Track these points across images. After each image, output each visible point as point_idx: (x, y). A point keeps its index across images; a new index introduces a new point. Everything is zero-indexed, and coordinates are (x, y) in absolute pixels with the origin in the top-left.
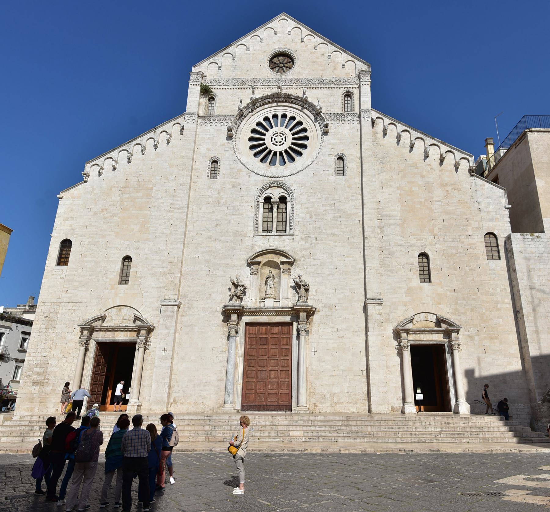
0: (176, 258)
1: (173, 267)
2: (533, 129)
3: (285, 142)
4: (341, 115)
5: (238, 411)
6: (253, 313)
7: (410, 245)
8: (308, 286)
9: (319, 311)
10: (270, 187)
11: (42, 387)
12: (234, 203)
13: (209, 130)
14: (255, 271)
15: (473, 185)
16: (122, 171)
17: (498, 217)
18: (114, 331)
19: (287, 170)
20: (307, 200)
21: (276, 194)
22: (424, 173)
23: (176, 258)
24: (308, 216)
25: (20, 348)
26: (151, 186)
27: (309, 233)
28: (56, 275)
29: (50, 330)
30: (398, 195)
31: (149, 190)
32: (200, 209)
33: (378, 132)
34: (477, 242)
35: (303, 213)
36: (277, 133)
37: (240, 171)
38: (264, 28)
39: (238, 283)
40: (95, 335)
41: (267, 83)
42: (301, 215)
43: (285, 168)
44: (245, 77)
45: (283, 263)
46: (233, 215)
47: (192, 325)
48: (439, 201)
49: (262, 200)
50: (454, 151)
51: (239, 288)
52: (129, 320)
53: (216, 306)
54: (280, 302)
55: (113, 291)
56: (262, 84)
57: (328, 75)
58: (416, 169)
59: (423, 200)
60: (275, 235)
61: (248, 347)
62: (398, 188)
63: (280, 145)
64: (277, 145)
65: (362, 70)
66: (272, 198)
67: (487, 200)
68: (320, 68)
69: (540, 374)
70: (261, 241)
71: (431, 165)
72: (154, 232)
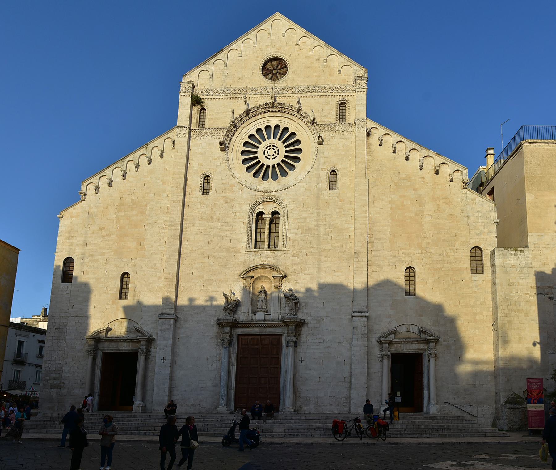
0: (171, 275)
1: (169, 283)
2: (529, 141)
3: (278, 155)
4: (335, 125)
5: (232, 412)
7: (398, 259)
8: (297, 300)
9: (307, 323)
10: (263, 202)
11: (59, 390)
12: (227, 219)
13: (201, 143)
14: (247, 286)
15: (465, 198)
16: (116, 189)
17: (486, 231)
18: (117, 342)
19: (279, 185)
20: (299, 216)
21: (267, 209)
22: (417, 187)
23: (171, 275)
25: (39, 355)
26: (145, 203)
27: (301, 248)
28: (62, 291)
29: (61, 341)
30: (390, 209)
31: (143, 208)
32: (193, 226)
33: (373, 144)
34: (463, 256)
36: (270, 146)
37: (232, 186)
38: (257, 30)
40: (101, 345)
41: (260, 92)
42: (292, 231)
43: (278, 183)
44: (236, 85)
48: (430, 215)
49: (255, 216)
50: (448, 163)
52: (130, 332)
53: (210, 319)
54: (271, 316)
55: (114, 306)
56: (254, 93)
57: (324, 81)
58: (409, 183)
59: (414, 215)
60: (267, 251)
61: (240, 356)
62: (390, 202)
63: (273, 159)
64: (269, 159)
65: (359, 75)
66: (264, 214)
67: (477, 215)
68: (315, 74)
69: (506, 379)
70: (253, 257)
71: (424, 178)
72: (149, 249)
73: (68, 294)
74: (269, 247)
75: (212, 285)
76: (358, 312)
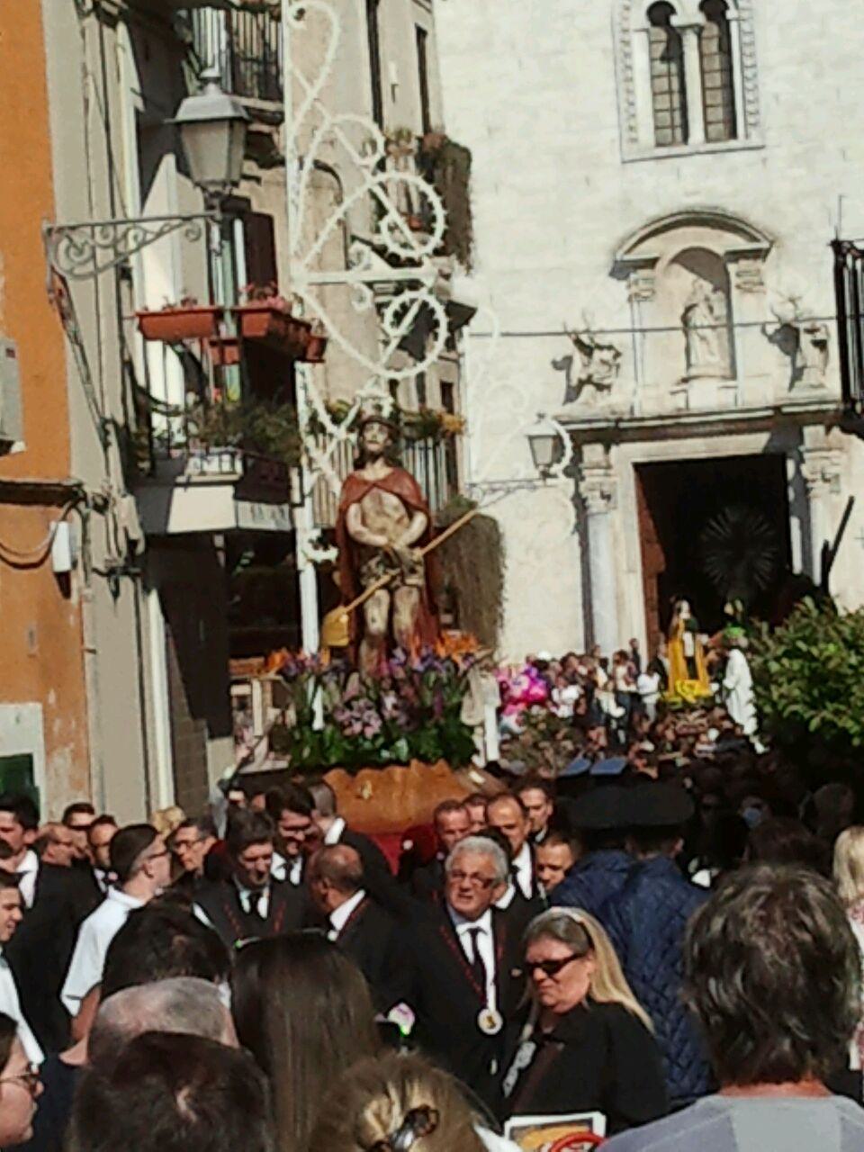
45: (736, 255)
49: (639, 18)
51: (597, 355)
74: (708, 139)
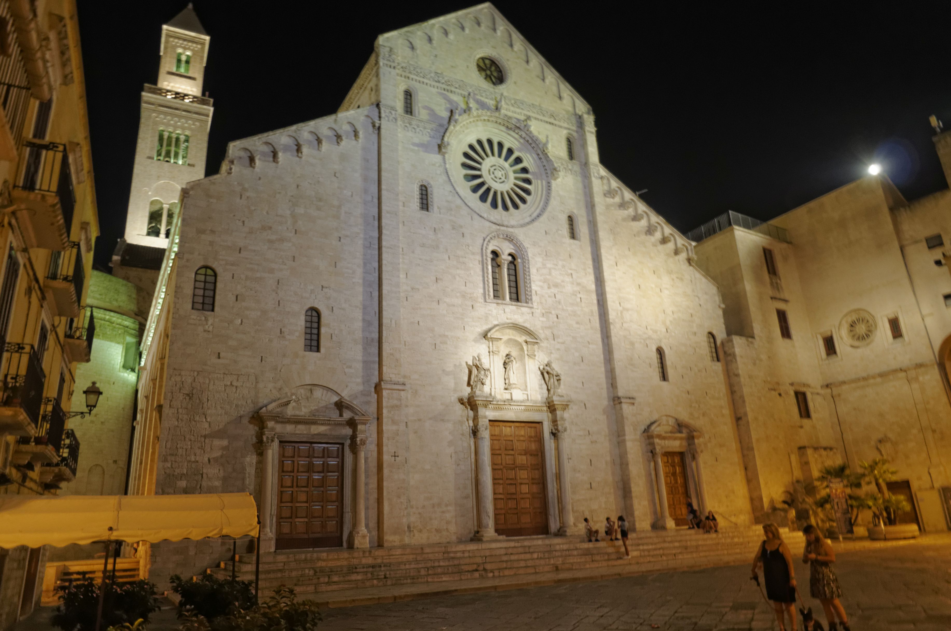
6: (498, 408)
24: (546, 286)
35: (540, 281)
39: (481, 365)
46: (458, 268)
47: (420, 420)
48: (667, 289)
73: (209, 331)
75: (447, 343)
76: (626, 398)
